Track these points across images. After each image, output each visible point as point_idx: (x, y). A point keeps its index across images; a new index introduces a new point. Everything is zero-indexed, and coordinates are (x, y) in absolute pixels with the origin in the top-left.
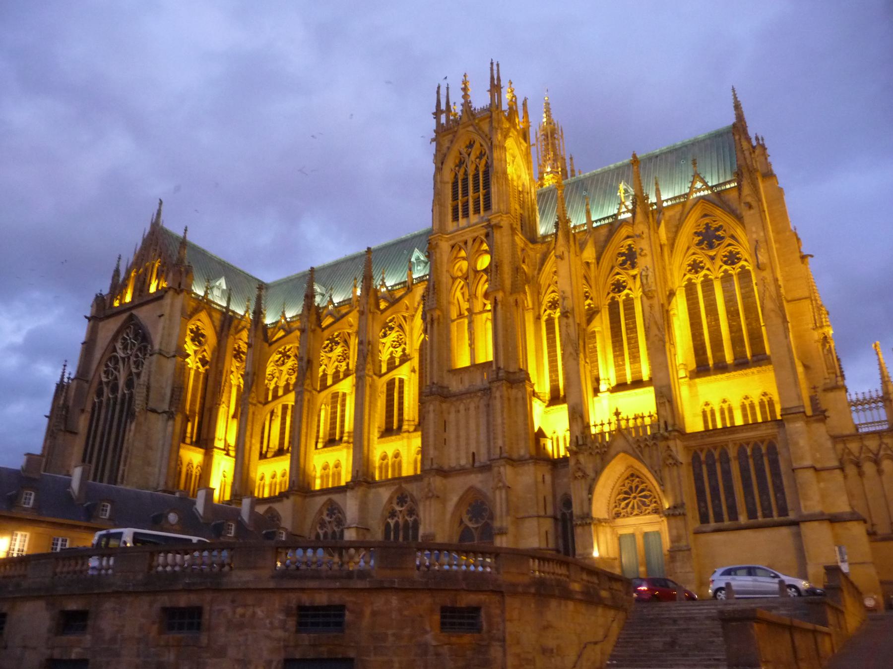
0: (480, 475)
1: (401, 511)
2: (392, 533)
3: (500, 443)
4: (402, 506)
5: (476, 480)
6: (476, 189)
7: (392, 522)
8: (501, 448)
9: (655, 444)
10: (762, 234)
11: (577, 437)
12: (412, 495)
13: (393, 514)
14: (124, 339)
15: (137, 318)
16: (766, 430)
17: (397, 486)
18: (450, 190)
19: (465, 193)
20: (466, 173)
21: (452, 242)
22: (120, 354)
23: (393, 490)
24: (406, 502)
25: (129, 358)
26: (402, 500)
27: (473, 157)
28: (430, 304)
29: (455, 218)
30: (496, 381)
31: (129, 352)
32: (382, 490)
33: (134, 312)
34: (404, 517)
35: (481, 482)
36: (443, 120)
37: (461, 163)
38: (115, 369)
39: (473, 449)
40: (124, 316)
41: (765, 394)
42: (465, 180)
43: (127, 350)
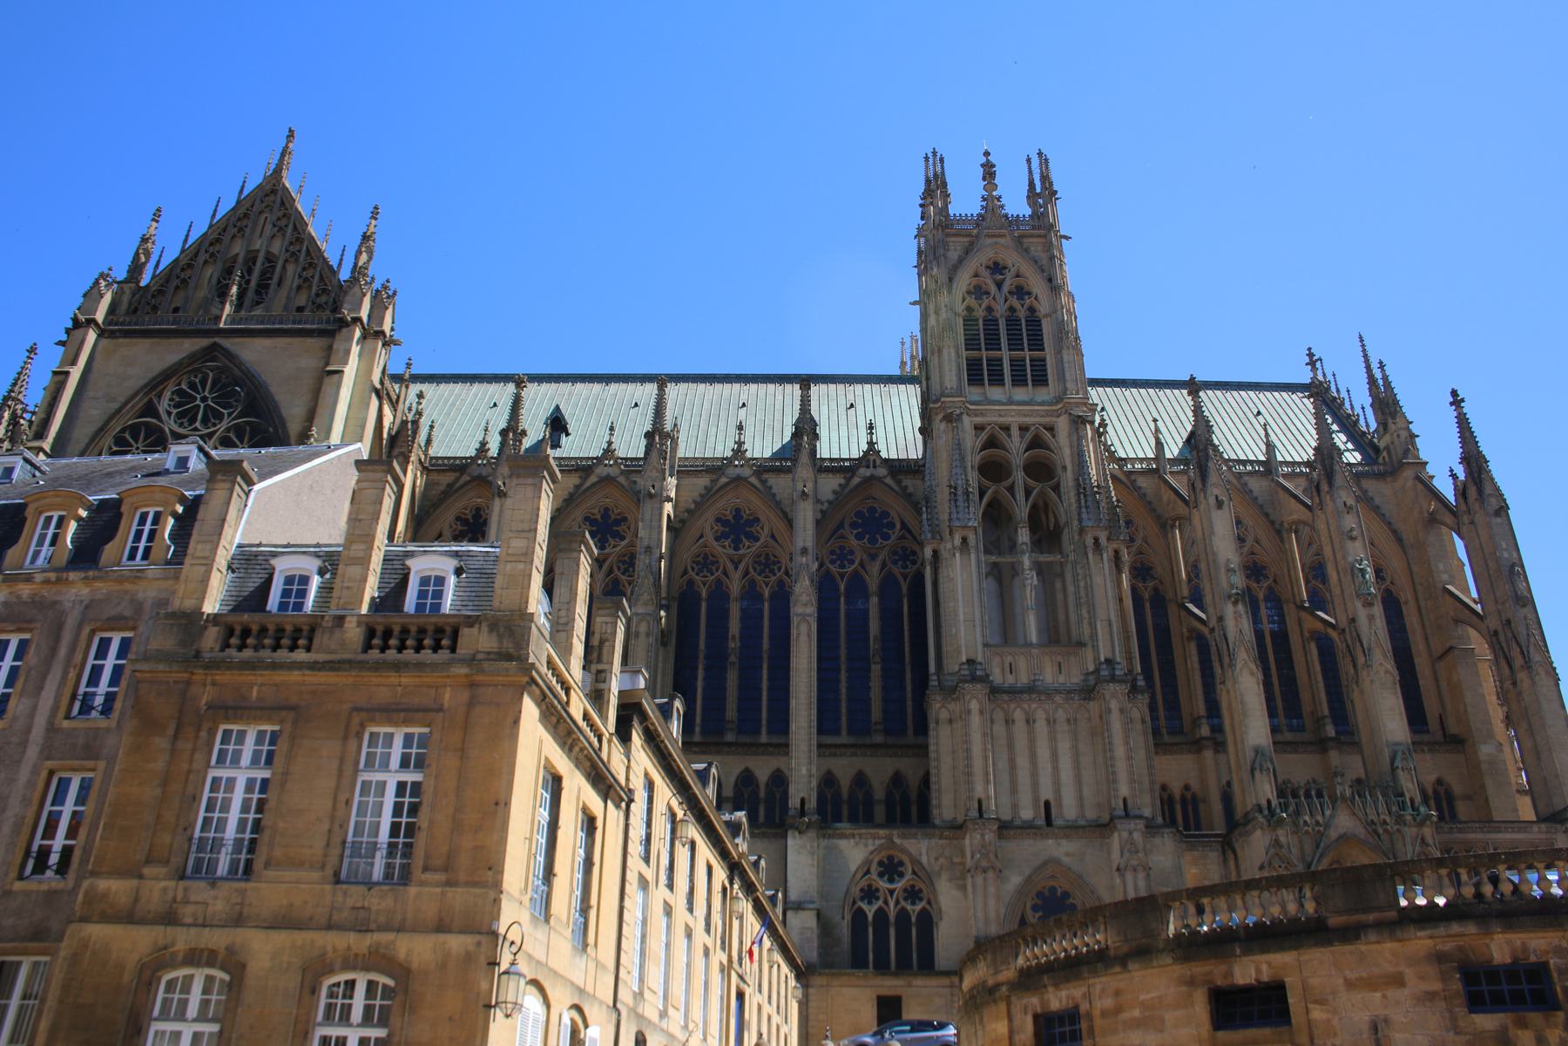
0: (1064, 842)
1: (892, 892)
2: (870, 930)
3: (1124, 790)
4: (891, 880)
5: (1061, 849)
6: (1015, 344)
7: (870, 911)
8: (1125, 800)
9: (1398, 831)
10: (1515, 555)
11: (1269, 802)
12: (916, 862)
13: (870, 894)
14: (180, 392)
16: (1540, 832)
17: (878, 842)
21: (979, 420)
23: (871, 848)
24: (901, 875)
26: (891, 868)
27: (1006, 288)
28: (960, 516)
30: (1108, 682)
32: (844, 844)
33: (226, 343)
34: (897, 902)
35: (1067, 854)
39: (1046, 793)
41: (1439, 782)
43: (193, 421)
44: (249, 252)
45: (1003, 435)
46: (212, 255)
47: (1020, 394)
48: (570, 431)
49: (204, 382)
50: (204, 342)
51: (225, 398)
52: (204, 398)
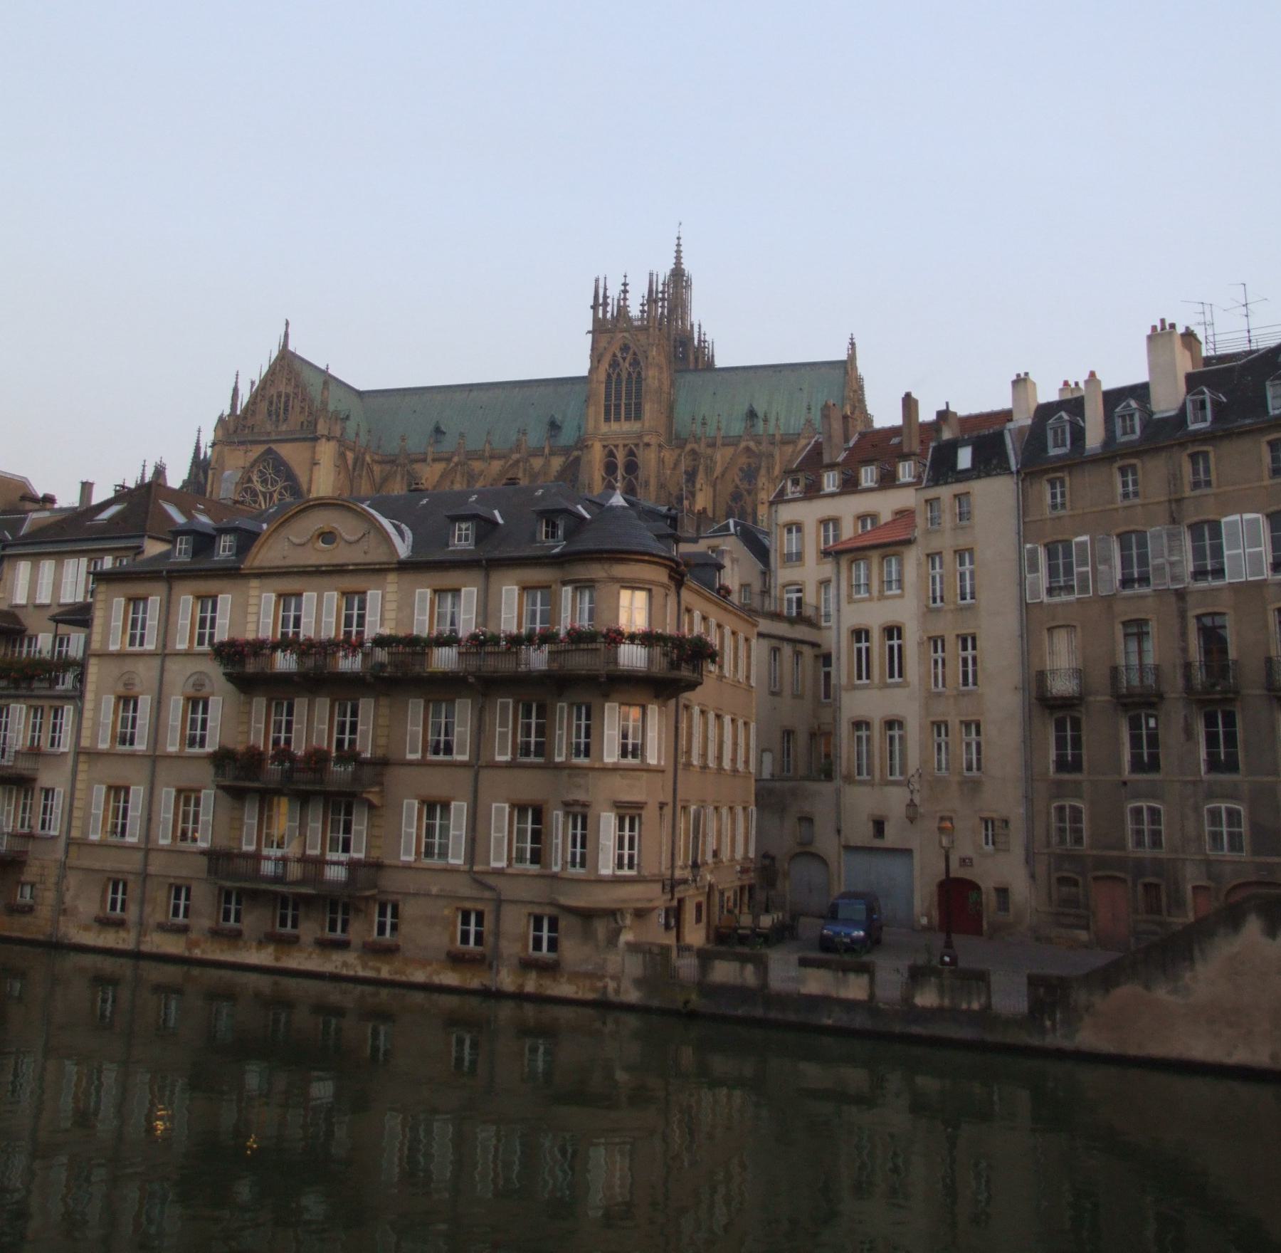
14: (260, 471)
15: (276, 453)
18: (604, 390)
19: (618, 397)
20: (619, 375)
21: (605, 443)
22: (259, 487)
25: (271, 497)
29: (607, 419)
31: (269, 486)
33: (274, 446)
36: (600, 315)
37: (614, 364)
38: (255, 502)
40: (261, 449)
42: (619, 382)
43: (267, 484)
44: (278, 393)
45: (615, 451)
46: (263, 396)
47: (626, 426)
48: (445, 430)
49: (268, 464)
50: (265, 447)
51: (277, 471)
52: (270, 474)
